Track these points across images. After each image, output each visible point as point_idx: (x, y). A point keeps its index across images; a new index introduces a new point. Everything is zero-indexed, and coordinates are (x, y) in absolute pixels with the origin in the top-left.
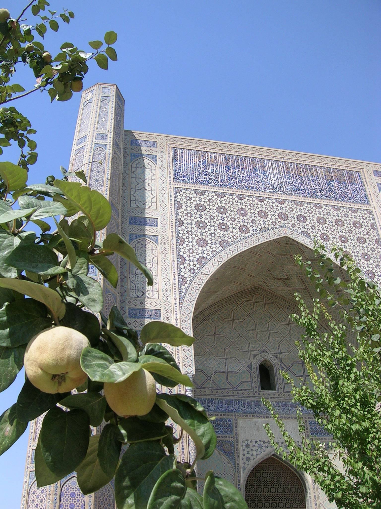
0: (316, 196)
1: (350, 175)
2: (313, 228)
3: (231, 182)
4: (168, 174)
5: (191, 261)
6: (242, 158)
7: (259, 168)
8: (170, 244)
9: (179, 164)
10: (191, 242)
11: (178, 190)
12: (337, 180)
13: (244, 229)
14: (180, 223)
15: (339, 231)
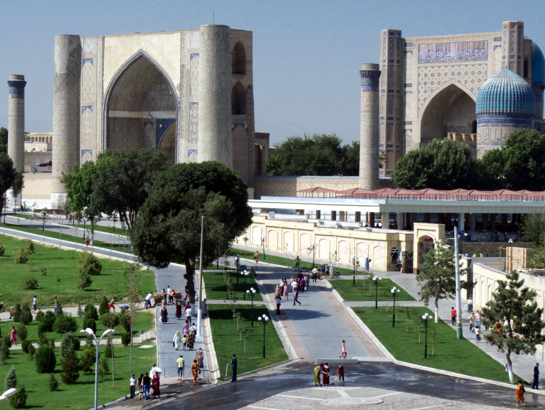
0: (467, 60)
1: (484, 43)
2: (463, 78)
3: (437, 59)
4: (416, 59)
5: (422, 99)
6: (442, 44)
7: (448, 49)
8: (415, 94)
9: (420, 53)
10: (422, 91)
11: (419, 68)
12: (477, 49)
13: (439, 83)
14: (419, 84)
15: (472, 77)
